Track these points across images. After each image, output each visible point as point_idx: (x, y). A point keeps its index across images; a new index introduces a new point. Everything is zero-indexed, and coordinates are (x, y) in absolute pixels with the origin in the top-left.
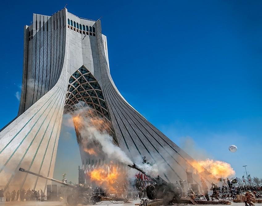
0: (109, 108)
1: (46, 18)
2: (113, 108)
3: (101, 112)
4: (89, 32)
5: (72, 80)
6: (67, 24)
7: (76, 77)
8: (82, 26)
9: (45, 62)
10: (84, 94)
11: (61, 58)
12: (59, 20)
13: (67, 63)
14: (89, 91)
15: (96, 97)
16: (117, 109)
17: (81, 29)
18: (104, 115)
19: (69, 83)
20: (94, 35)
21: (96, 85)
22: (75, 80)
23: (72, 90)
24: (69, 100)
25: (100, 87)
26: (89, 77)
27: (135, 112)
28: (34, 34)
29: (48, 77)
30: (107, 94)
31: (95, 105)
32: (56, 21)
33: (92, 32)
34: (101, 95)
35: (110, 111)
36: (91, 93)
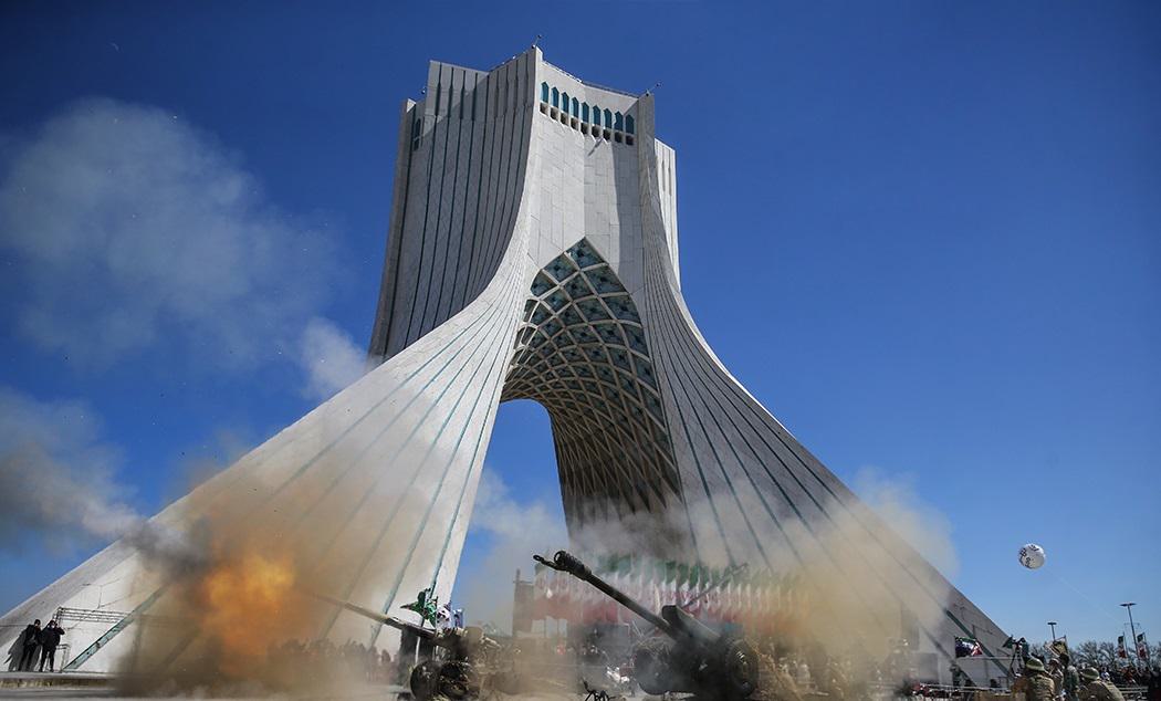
0: (664, 385)
1: (471, 78)
3: (638, 399)
4: (612, 132)
5: (540, 284)
6: (538, 100)
7: (557, 276)
8: (591, 111)
9: (458, 221)
10: (584, 335)
12: (512, 86)
13: (528, 229)
14: (600, 325)
15: (621, 347)
16: (690, 390)
17: (586, 118)
19: (531, 295)
20: (630, 141)
21: (625, 307)
22: (555, 285)
23: (543, 319)
24: (529, 352)
25: (637, 315)
27: (749, 404)
28: (427, 128)
29: (463, 272)
30: (660, 339)
32: (502, 90)
33: (623, 132)
34: (638, 339)
35: (667, 397)
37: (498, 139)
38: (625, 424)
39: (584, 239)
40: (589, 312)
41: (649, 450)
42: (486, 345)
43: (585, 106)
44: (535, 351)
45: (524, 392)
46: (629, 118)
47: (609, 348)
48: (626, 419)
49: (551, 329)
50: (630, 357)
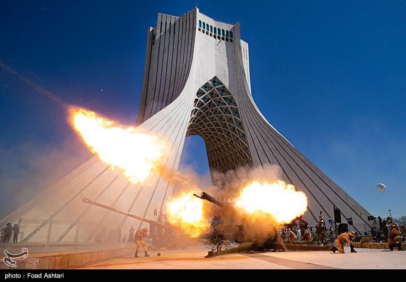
0: (246, 129)
1: (173, 19)
2: (251, 129)
3: (236, 134)
4: (225, 37)
5: (200, 93)
6: (198, 27)
7: (206, 90)
9: (169, 70)
10: (216, 111)
11: (187, 66)
12: (188, 22)
16: (256, 130)
17: (215, 33)
18: (240, 137)
19: (197, 97)
20: (231, 41)
21: (231, 101)
24: (196, 118)
25: (235, 103)
26: (223, 91)
28: (157, 37)
30: (244, 112)
31: (229, 125)
32: (184, 23)
33: (229, 38)
34: (236, 113)
36: (226, 110)
37: (183, 40)
38: (232, 143)
39: (215, 77)
40: (218, 103)
41: (241, 152)
42: (180, 115)
43: (215, 28)
44: (199, 118)
45: (195, 133)
46: (231, 32)
47: (225, 116)
48: (232, 142)
49: (204, 109)
50: (233, 118)
